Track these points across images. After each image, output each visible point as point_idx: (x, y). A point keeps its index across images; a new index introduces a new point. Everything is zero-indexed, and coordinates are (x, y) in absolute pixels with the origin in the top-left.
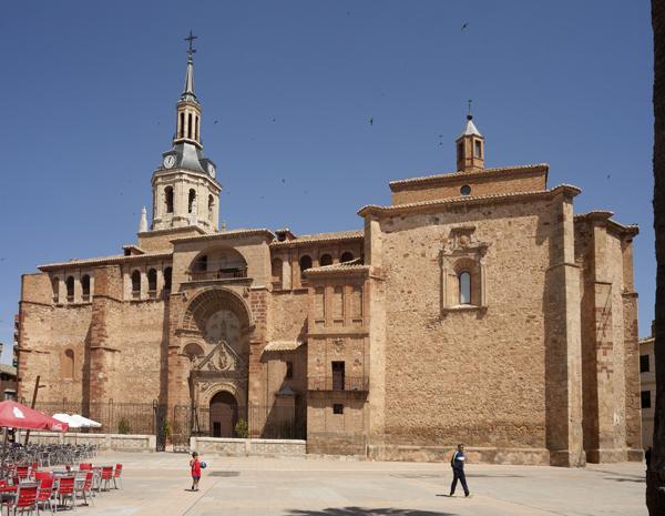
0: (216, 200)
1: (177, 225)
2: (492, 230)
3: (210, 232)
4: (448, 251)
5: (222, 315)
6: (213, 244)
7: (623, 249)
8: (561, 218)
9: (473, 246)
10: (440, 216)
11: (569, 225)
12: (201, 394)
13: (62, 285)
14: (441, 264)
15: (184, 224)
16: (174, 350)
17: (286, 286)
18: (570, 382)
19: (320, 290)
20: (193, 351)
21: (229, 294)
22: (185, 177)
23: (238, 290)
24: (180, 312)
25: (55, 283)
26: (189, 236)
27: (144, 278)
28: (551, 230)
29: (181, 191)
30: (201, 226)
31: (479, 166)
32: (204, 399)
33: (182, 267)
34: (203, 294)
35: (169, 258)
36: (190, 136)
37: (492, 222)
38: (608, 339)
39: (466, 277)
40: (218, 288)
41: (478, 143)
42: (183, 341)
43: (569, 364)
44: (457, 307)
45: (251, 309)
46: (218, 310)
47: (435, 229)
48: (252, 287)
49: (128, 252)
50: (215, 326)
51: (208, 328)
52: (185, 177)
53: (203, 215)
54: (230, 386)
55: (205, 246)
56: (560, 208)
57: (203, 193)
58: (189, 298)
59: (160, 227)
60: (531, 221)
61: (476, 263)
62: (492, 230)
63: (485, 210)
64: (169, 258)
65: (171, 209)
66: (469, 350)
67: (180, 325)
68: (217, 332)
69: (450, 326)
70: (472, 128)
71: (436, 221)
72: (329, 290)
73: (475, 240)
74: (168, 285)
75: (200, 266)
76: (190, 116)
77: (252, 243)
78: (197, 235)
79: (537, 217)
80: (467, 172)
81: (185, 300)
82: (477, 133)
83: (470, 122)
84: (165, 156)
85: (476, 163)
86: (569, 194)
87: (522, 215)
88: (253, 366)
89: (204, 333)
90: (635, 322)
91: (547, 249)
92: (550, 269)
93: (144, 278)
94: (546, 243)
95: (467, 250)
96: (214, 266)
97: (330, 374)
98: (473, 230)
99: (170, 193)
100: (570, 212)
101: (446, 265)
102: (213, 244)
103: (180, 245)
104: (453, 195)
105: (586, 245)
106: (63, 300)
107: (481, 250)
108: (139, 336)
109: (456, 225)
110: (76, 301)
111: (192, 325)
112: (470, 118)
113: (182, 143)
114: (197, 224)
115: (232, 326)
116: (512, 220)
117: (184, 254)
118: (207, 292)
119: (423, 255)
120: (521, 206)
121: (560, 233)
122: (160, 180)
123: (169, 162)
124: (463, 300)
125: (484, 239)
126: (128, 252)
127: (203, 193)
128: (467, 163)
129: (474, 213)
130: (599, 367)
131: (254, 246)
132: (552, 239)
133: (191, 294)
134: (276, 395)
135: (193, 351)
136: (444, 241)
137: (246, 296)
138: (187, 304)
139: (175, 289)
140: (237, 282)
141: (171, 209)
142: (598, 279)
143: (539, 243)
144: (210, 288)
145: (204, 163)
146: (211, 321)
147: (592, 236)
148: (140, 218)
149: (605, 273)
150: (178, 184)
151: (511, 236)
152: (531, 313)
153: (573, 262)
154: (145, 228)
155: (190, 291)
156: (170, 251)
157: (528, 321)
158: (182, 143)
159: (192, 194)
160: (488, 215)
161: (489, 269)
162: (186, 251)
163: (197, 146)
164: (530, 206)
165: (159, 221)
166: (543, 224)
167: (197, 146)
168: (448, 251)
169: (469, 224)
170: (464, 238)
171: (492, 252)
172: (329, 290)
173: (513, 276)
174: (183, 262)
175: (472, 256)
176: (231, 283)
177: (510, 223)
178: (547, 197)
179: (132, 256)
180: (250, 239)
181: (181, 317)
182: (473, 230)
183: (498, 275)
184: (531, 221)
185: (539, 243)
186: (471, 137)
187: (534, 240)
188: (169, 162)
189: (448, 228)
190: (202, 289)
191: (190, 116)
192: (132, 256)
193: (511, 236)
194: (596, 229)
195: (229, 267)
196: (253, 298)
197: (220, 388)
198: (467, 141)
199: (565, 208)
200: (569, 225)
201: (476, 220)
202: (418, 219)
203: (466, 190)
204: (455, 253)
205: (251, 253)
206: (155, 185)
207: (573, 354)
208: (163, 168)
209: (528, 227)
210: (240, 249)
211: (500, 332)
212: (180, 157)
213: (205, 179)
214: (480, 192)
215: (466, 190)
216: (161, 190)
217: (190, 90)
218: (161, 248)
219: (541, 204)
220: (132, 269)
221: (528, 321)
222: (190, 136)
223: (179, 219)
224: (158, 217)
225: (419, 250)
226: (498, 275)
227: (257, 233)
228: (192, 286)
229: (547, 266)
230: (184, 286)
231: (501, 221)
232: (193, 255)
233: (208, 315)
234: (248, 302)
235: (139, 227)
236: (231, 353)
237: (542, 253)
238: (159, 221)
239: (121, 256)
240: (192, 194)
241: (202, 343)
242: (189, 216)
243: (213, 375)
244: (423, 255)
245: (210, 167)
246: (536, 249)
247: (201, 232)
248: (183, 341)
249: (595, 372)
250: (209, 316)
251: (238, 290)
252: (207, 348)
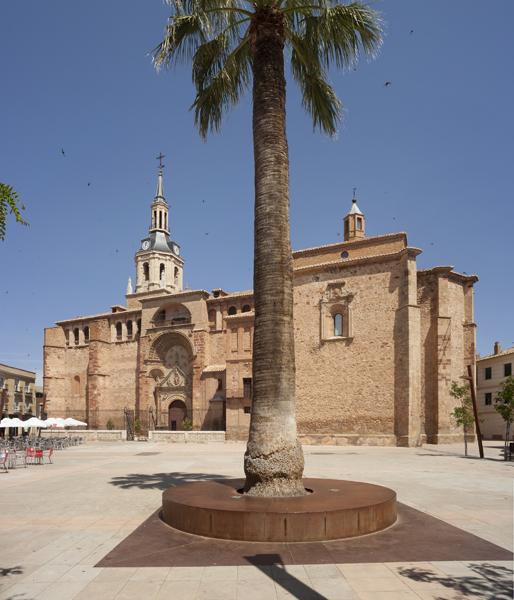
0: (180, 270)
1: (152, 289)
2: (357, 284)
3: (174, 292)
4: (325, 300)
5: (176, 349)
6: (168, 301)
7: (465, 293)
8: (407, 273)
9: (342, 295)
10: (320, 276)
11: (413, 278)
12: (163, 403)
13: (71, 333)
14: (320, 309)
15: (157, 288)
17: (219, 328)
18: (410, 389)
19: (234, 330)
20: (156, 374)
21: (180, 336)
22: (157, 255)
23: (185, 332)
24: (147, 347)
25: (66, 333)
26: (156, 296)
27: (124, 327)
28: (400, 282)
29: (154, 265)
30: (169, 289)
31: (360, 236)
32: (165, 405)
35: (140, 313)
36: (160, 227)
37: (357, 278)
38: (447, 357)
39: (338, 317)
40: (172, 331)
41: (360, 220)
42: (149, 368)
43: (410, 376)
44: (332, 338)
46: (173, 346)
47: (317, 285)
49: (114, 310)
50: (171, 357)
52: (157, 255)
53: (169, 280)
54: (181, 397)
55: (162, 303)
56: (406, 265)
57: (170, 266)
59: (140, 291)
60: (384, 277)
61: (345, 307)
62: (357, 284)
63: (352, 270)
64: (140, 313)
65: (147, 278)
66: (340, 367)
67: (147, 357)
68: (174, 360)
69: (326, 351)
70: (355, 209)
71: (317, 279)
72: (241, 330)
73: (344, 291)
74: (139, 332)
75: (160, 317)
76: (161, 212)
78: (165, 294)
79: (390, 273)
80: (351, 241)
82: (359, 212)
83: (355, 205)
84: (143, 241)
85: (358, 234)
86: (412, 254)
87: (379, 272)
88: (195, 382)
89: (164, 362)
90: (473, 344)
91: (397, 296)
92: (398, 310)
93: (124, 327)
94: (397, 291)
95: (339, 298)
96: (170, 317)
97: (242, 386)
98: (343, 284)
99: (147, 267)
100: (413, 267)
101: (324, 309)
102: (168, 301)
103: (146, 303)
104: (336, 259)
105: (432, 291)
106: (72, 344)
107: (349, 298)
108: (122, 366)
109: (331, 282)
110: (80, 344)
111: (155, 357)
112: (354, 201)
113: (155, 232)
114: (165, 288)
115: (182, 356)
116: (372, 276)
117: (149, 310)
119: (308, 303)
120: (378, 265)
121: (406, 284)
122: (139, 258)
123: (146, 246)
124: (337, 333)
125: (353, 291)
126: (114, 310)
127: (170, 266)
128: (351, 234)
129: (343, 273)
130: (439, 377)
132: (401, 288)
133: (154, 336)
134: (210, 402)
135: (156, 374)
136: (322, 293)
137: (190, 336)
138: (151, 343)
139: (143, 334)
140: (185, 327)
141: (147, 278)
142: (440, 315)
143: (391, 291)
144: (166, 331)
145: (171, 245)
146: (169, 354)
147: (437, 284)
148: (127, 284)
149: (446, 310)
150: (152, 261)
151: (371, 287)
152: (385, 341)
153: (416, 304)
154: (130, 292)
156: (140, 309)
157: (382, 347)
158: (155, 232)
159: (162, 267)
160: (354, 274)
161: (355, 312)
162: (150, 307)
163: (166, 234)
164: (385, 266)
165: (140, 287)
166: (395, 278)
167: (166, 234)
168: (325, 300)
169: (341, 280)
170: (337, 290)
171: (357, 299)
172: (241, 330)
173: (372, 315)
174: (148, 315)
175: (342, 302)
176: (181, 327)
177: (370, 278)
178: (397, 258)
179: (118, 312)
181: (147, 352)
182: (343, 284)
183: (361, 316)
184: (384, 277)
185: (391, 291)
186: (354, 215)
187: (387, 290)
188: (146, 246)
189: (326, 283)
190: (161, 333)
191: (161, 212)
192: (118, 312)
193: (371, 287)
194: (440, 279)
195: (181, 317)
198: (351, 218)
199: (409, 264)
200: (413, 278)
201: (345, 277)
202: (304, 278)
203: (345, 255)
204: (331, 301)
206: (137, 262)
207: (413, 369)
208: (142, 250)
209: (384, 281)
210: (186, 304)
211: (362, 355)
212: (153, 242)
213: (171, 256)
214: (354, 256)
215: (345, 255)
216: (141, 265)
217: (160, 194)
218: (131, 307)
219: (393, 264)
220: (116, 322)
221: (382, 347)
222: (160, 227)
223: (153, 284)
224: (139, 284)
225: (305, 300)
226: (361, 316)
227: (197, 293)
228: (154, 330)
229: (397, 307)
230: (149, 331)
231: (364, 277)
232: (155, 309)
233: (167, 349)
234: (192, 340)
235: (126, 291)
237: (394, 297)
238: (140, 287)
239: (110, 313)
240: (162, 267)
241: (163, 368)
242: (160, 282)
243: (170, 390)
244: (308, 303)
245: (175, 248)
246: (389, 295)
247: (168, 293)
248: (149, 368)
249: (436, 381)
251: (185, 332)
252: (166, 371)
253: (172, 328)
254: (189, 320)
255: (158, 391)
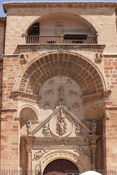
5: (59, 80)
6: (55, 10)
12: (35, 163)
16: (8, 114)
21: (76, 58)
23: (89, 55)
33: (19, 30)
34: (46, 57)
40: (64, 52)
42: (20, 105)
45: (104, 75)
46: (56, 75)
48: (105, 53)
50: (50, 92)
51: (42, 93)
55: (46, 12)
58: (28, 60)
67: (16, 88)
68: (55, 98)
77: (102, 14)
81: (25, 62)
89: (37, 97)
102: (55, 10)
111: (27, 88)
115: (72, 92)
117: (20, 18)
118: (51, 55)
131: (104, 17)
137: (99, 61)
138: (26, 67)
140: (88, 47)
146: (45, 87)
155: (29, 53)
162: (23, 15)
180: (99, 10)
196: (105, 64)
197: (58, 156)
205: (101, 22)
210: (89, 18)
227: (107, 5)
232: (29, 20)
233: (44, 80)
234: (101, 68)
236: (72, 120)
241: (36, 107)
250: (45, 80)
251: (89, 55)
252: (42, 114)
253: (66, 47)
254: (95, 39)
255: (26, 143)
